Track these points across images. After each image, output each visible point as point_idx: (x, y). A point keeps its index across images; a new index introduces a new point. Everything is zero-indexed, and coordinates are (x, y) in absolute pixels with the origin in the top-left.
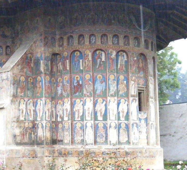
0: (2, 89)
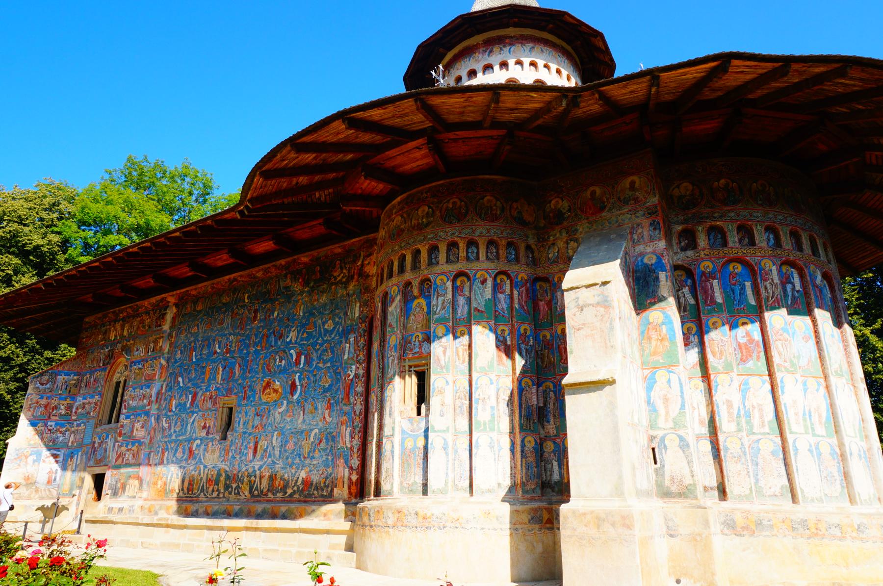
0: (581, 332)
